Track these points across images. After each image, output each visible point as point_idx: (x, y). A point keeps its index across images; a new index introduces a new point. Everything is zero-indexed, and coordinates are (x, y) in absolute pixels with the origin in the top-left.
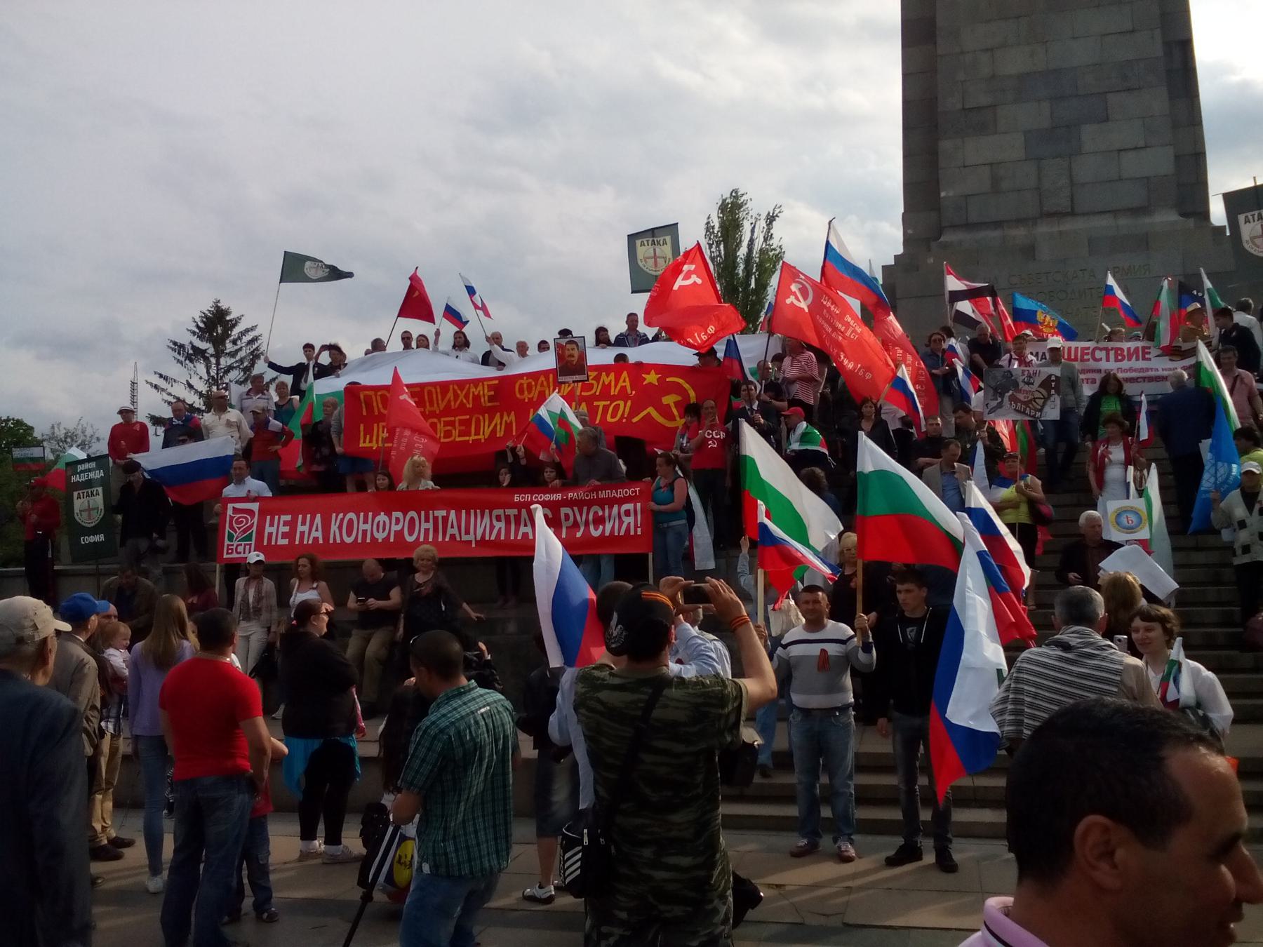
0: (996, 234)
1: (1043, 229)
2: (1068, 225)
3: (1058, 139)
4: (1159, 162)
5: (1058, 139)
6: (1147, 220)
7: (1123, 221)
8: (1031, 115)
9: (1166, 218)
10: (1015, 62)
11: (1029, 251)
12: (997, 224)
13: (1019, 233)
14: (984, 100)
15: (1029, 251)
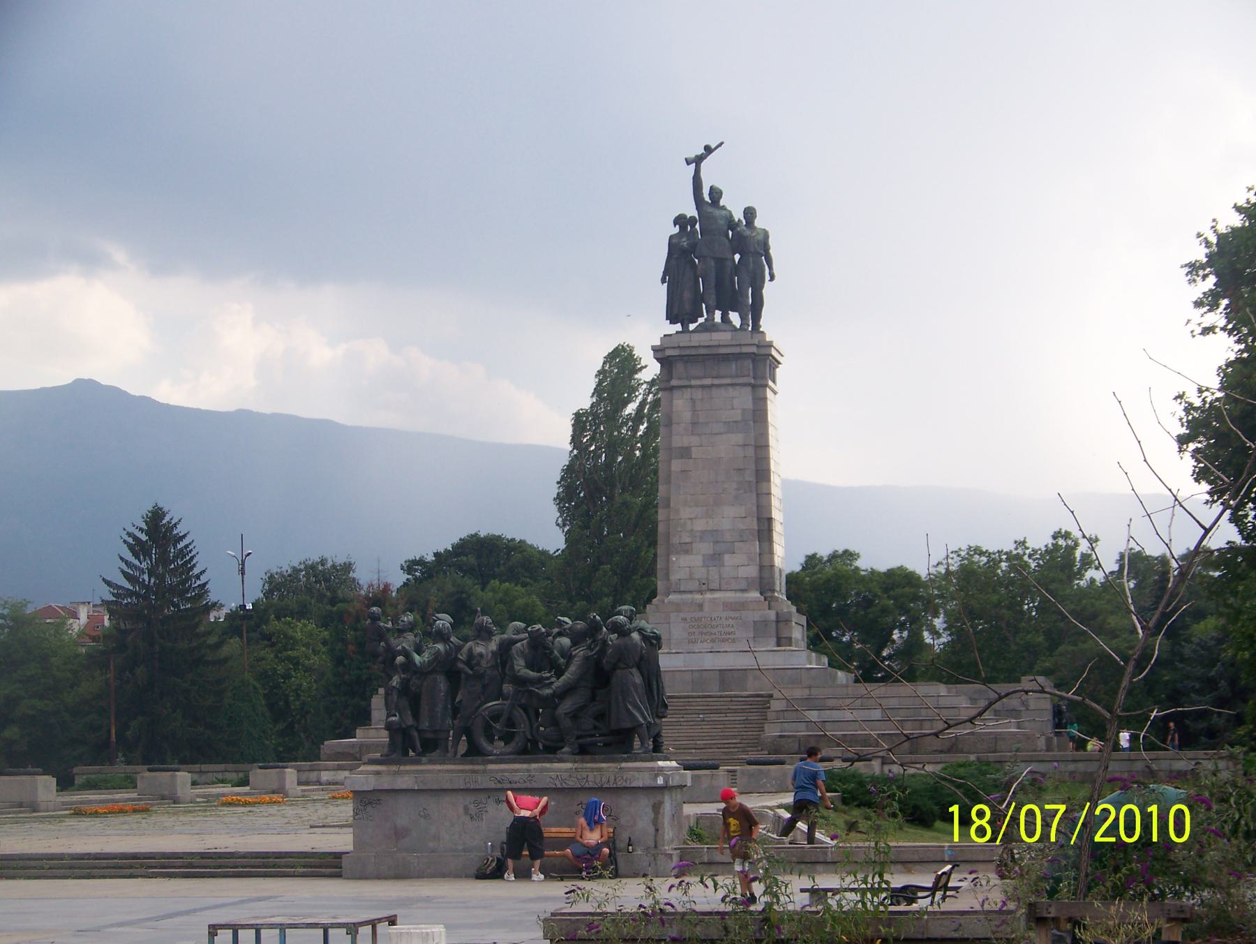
0: (689, 596)
1: (708, 596)
2: (717, 595)
3: (715, 559)
4: (752, 571)
5: (715, 559)
6: (746, 595)
7: (739, 594)
8: (705, 548)
9: (755, 595)
10: (700, 525)
11: (701, 606)
12: (691, 592)
13: (698, 597)
14: (688, 540)
15: (701, 606)
